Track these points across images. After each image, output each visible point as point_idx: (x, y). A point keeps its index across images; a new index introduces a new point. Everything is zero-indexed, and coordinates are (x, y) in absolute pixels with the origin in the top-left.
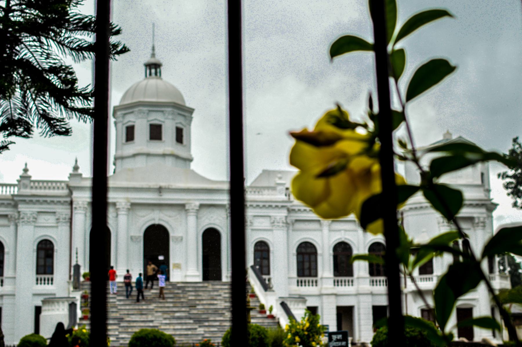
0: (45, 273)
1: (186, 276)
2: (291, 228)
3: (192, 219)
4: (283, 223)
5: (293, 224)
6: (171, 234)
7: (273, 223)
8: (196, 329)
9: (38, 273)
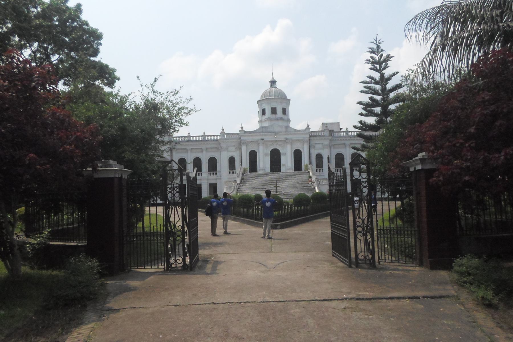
0: (233, 170)
2: (332, 148)
3: (289, 147)
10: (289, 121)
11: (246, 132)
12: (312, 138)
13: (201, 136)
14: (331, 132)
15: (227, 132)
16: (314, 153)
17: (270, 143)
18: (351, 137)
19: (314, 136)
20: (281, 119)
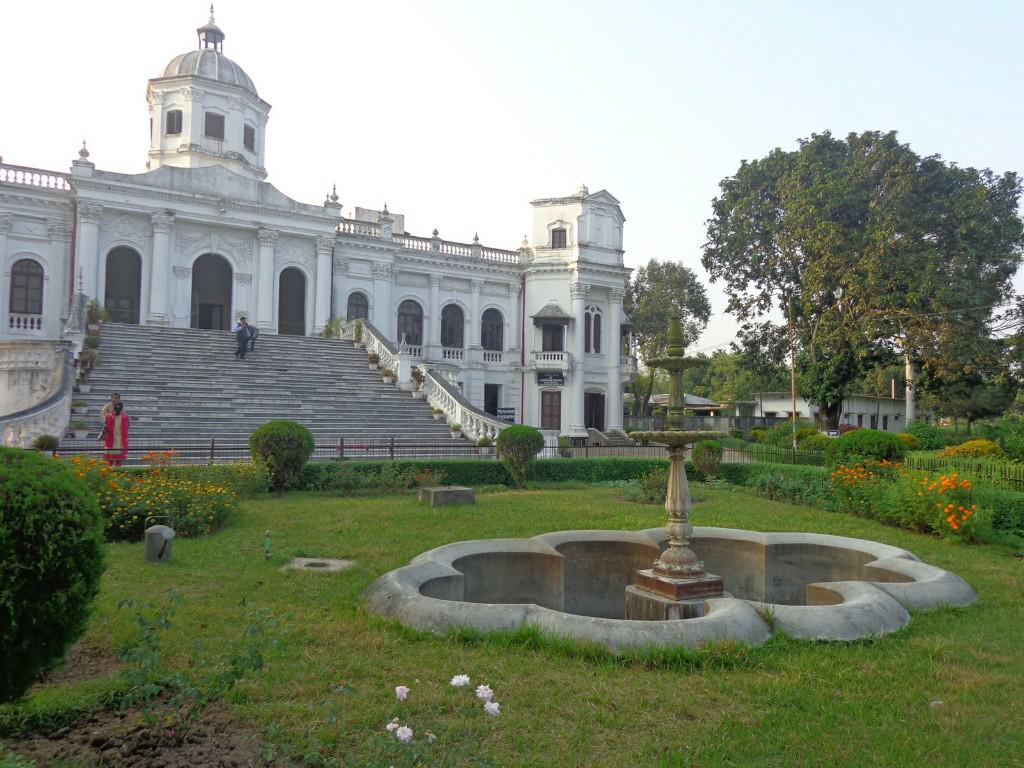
3: (266, 253)
6: (236, 270)
8: (299, 406)
9: (11, 311)
11: (101, 173)
12: (344, 241)
16: (347, 287)
18: (448, 257)
20: (241, 159)
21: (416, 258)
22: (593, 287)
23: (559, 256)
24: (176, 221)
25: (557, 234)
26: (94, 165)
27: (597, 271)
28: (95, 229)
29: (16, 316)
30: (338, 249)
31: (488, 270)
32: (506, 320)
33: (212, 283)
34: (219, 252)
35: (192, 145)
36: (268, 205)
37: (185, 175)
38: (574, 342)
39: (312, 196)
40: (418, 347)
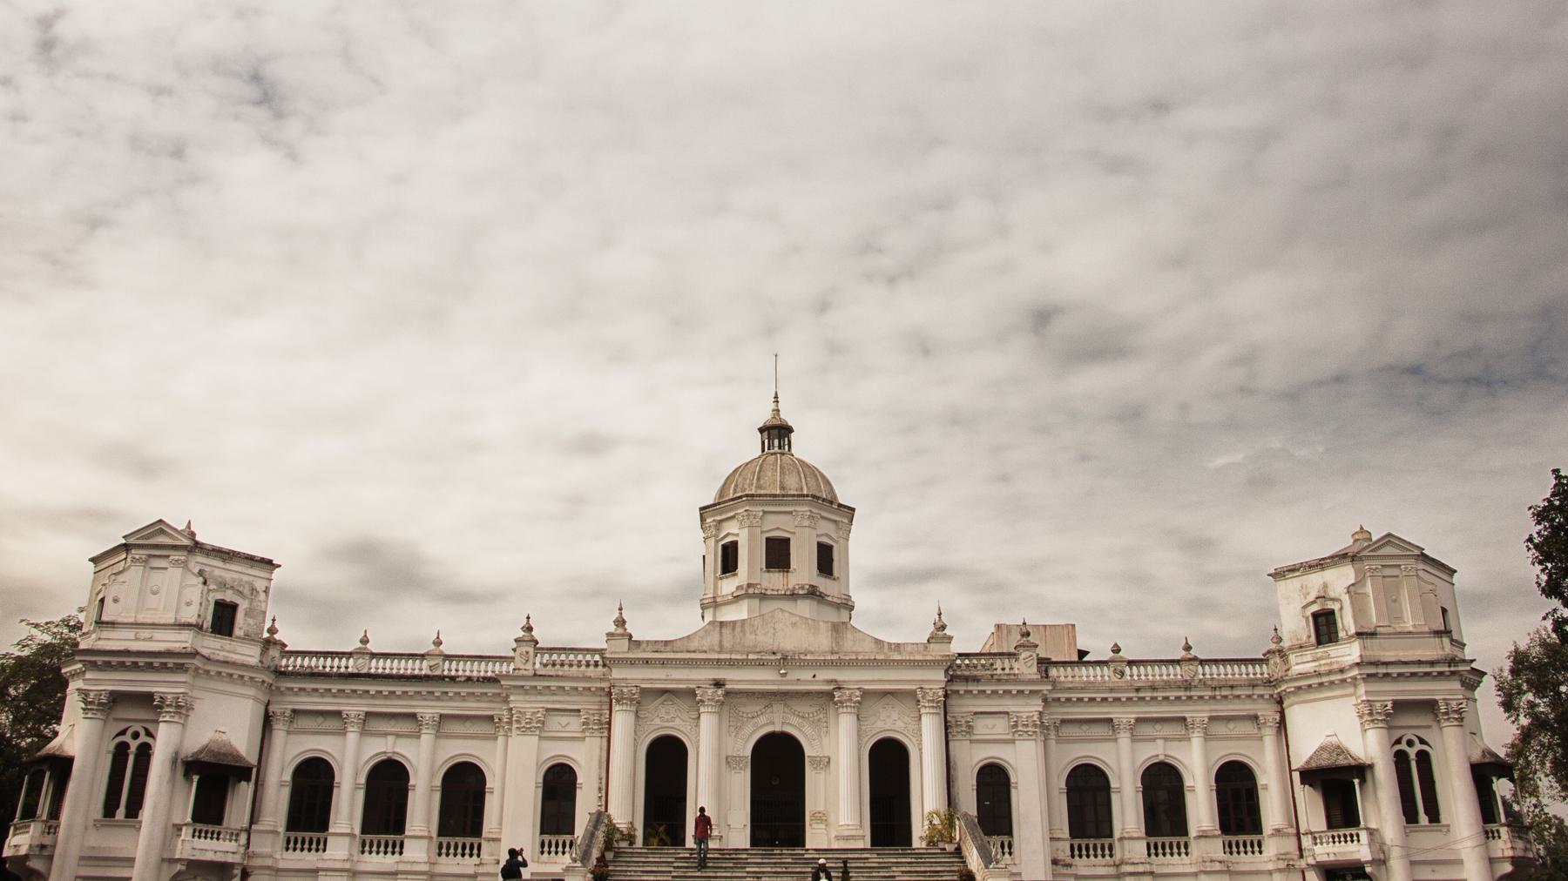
0: (558, 832)
1: (837, 838)
4: (1035, 726)
5: (1057, 729)
6: (808, 752)
7: (1016, 725)
9: (542, 832)
10: (848, 606)
11: (638, 643)
12: (961, 688)
13: (423, 656)
14: (1045, 664)
15: (543, 636)
16: (971, 759)
17: (753, 707)
19: (966, 679)
20: (813, 593)
21: (1086, 696)
22: (1400, 706)
23: (1328, 657)
24: (728, 693)
25: (1322, 620)
26: (630, 636)
27: (1400, 675)
28: (632, 716)
29: (547, 838)
30: (953, 701)
31: (1214, 697)
32: (1261, 780)
33: (778, 772)
34: (788, 729)
35: (749, 585)
36: (846, 653)
37: (738, 629)
38: (1380, 807)
39: (912, 631)
40: (1106, 842)
